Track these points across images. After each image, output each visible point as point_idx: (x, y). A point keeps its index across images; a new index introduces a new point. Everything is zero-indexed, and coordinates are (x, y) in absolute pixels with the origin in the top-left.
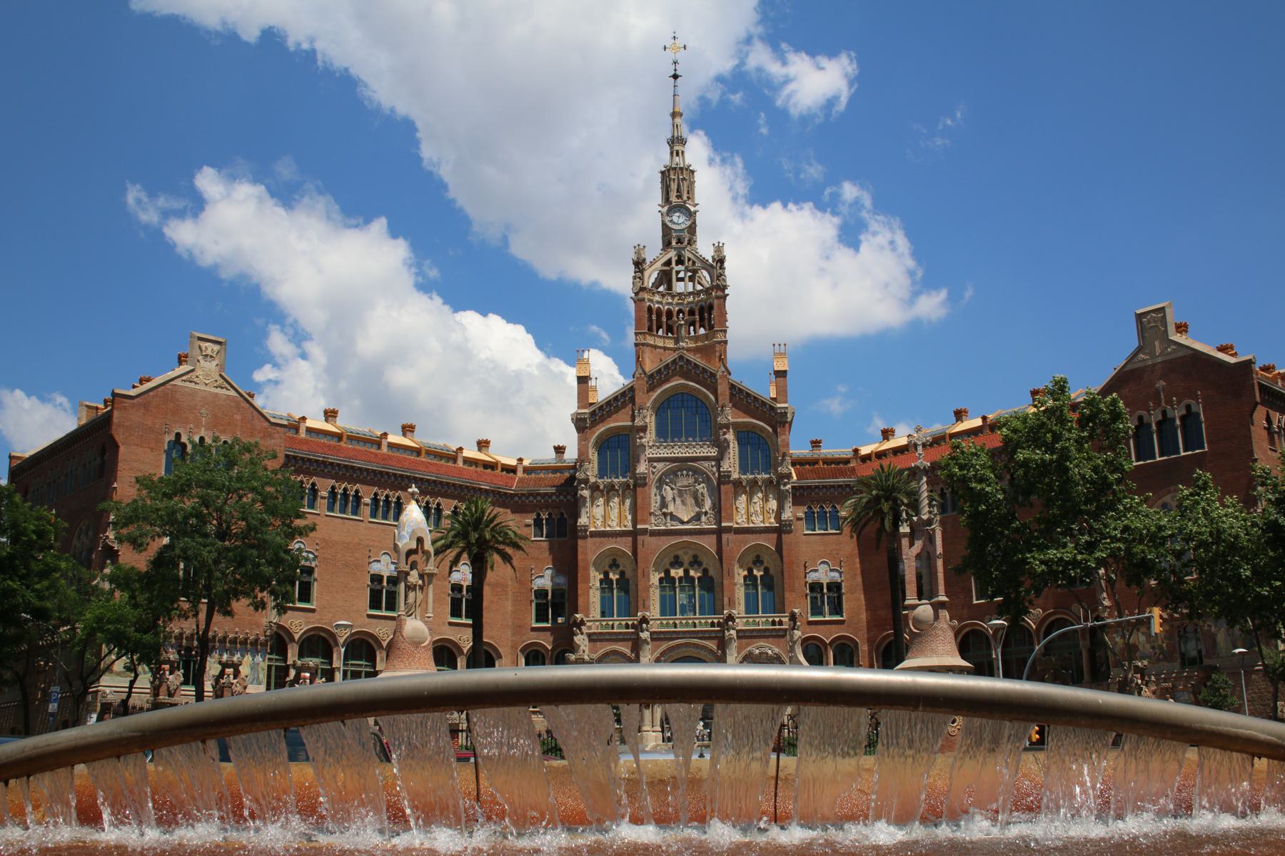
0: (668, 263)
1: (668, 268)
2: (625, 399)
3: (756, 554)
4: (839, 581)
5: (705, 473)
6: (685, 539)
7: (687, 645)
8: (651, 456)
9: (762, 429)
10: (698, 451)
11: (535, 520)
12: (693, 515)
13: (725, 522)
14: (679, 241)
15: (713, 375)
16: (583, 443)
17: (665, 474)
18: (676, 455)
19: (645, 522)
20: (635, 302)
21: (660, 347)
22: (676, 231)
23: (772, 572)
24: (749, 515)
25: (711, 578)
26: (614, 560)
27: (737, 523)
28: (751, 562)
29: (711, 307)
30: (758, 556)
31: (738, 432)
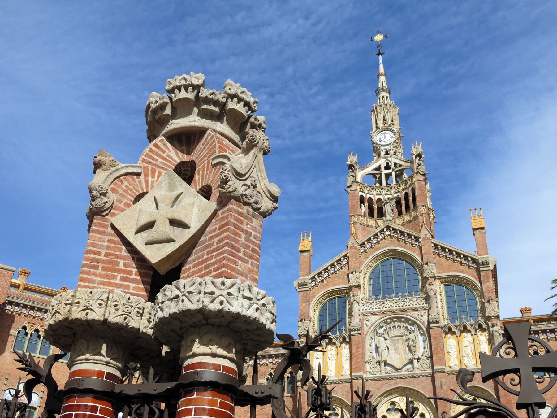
0: (378, 169)
1: (378, 172)
8: (365, 311)
10: (408, 304)
11: (268, 379)
13: (436, 366)
14: (387, 153)
15: (417, 239)
16: (304, 304)
18: (388, 308)
19: (359, 369)
21: (372, 227)
22: (382, 145)
24: (460, 358)
27: (450, 367)
29: (413, 191)
31: (445, 286)
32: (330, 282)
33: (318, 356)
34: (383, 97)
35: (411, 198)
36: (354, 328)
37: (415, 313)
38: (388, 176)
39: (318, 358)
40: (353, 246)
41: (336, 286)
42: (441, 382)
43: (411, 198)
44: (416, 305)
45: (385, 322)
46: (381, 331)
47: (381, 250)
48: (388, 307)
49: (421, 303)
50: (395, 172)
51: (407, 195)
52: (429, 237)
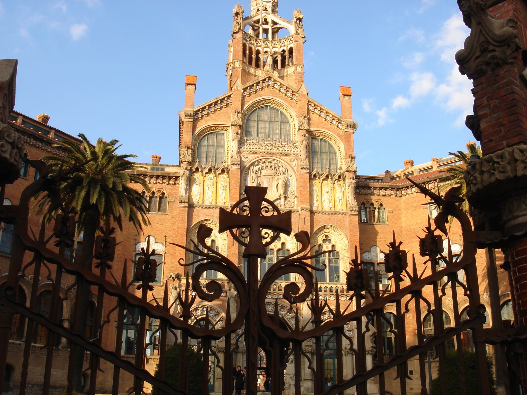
18: (263, 150)
23: (337, 249)
29: (291, 50)
32: (212, 118)
36: (235, 162)
37: (287, 158)
38: (266, 31)
40: (237, 89)
41: (218, 122)
42: (305, 218)
44: (282, 150)
45: (259, 161)
46: (256, 168)
47: (262, 98)
48: (263, 149)
49: (293, 150)
50: (272, 29)
51: (284, 51)
52: (304, 95)
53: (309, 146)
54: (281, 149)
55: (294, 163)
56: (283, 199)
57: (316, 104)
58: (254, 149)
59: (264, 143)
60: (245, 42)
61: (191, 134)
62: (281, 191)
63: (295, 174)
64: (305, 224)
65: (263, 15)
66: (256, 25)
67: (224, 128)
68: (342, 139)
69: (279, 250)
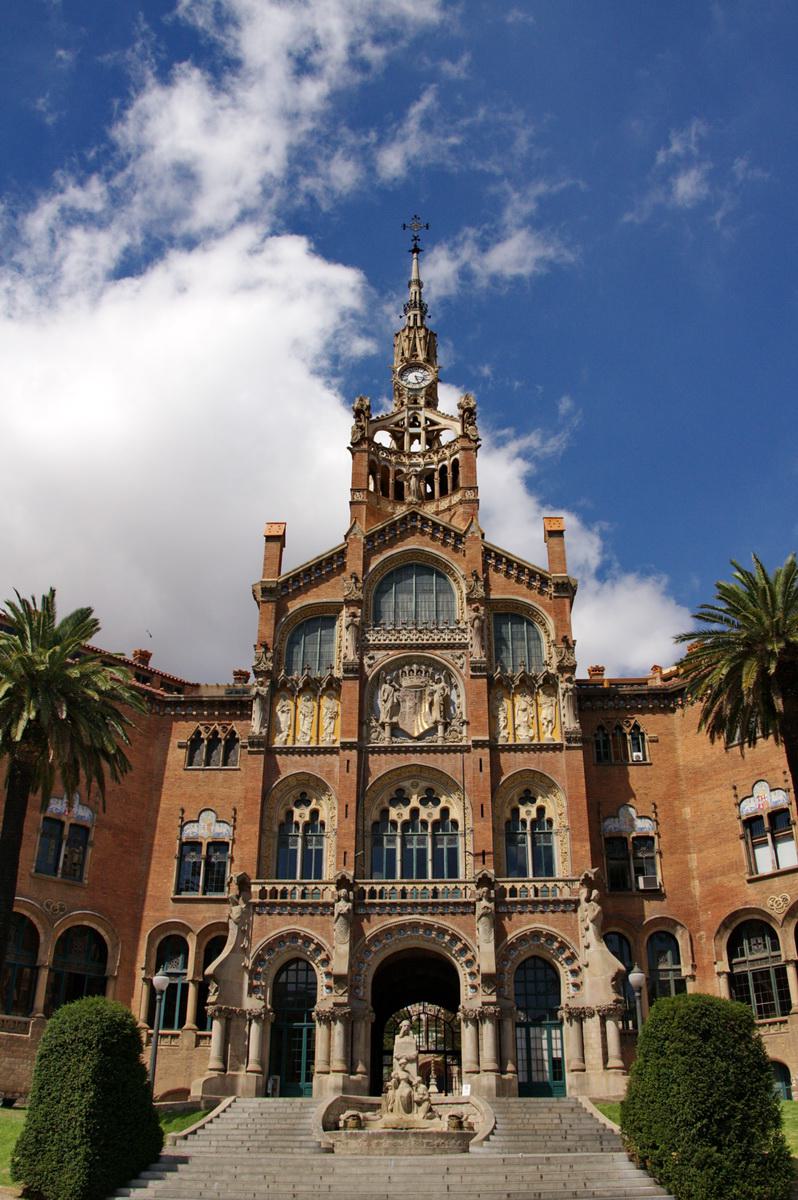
2: (329, 566)
3: (525, 787)
4: (652, 834)
5: (445, 667)
6: (415, 759)
7: (415, 926)
9: (529, 608)
11: (192, 740)
12: (426, 727)
17: (388, 668)
18: (403, 642)
20: (353, 454)
25: (455, 823)
26: (304, 794)
28: (516, 798)
29: (456, 463)
30: (527, 791)
33: (285, 709)
34: (415, 315)
35: (450, 475)
39: (283, 712)
42: (481, 760)
43: (450, 475)
49: (457, 637)
51: (444, 467)
53: (488, 629)
54: (436, 638)
55: (460, 662)
56: (440, 728)
57: (499, 552)
58: (387, 642)
59: (405, 629)
60: (372, 457)
61: (273, 622)
62: (436, 715)
63: (463, 680)
64: (481, 770)
65: (411, 412)
66: (397, 429)
67: (336, 608)
68: (549, 612)
69: (436, 825)
